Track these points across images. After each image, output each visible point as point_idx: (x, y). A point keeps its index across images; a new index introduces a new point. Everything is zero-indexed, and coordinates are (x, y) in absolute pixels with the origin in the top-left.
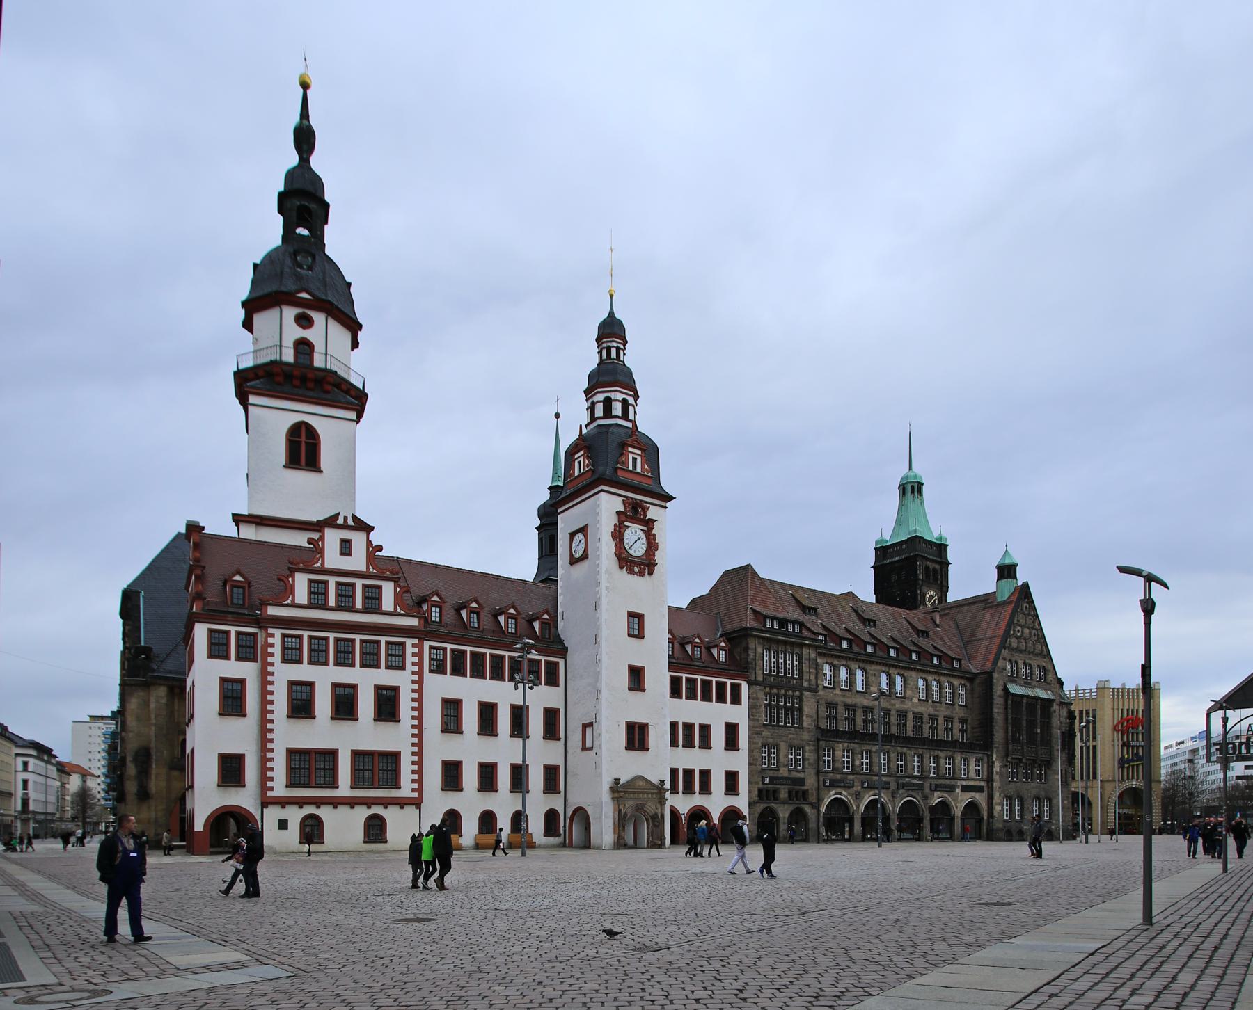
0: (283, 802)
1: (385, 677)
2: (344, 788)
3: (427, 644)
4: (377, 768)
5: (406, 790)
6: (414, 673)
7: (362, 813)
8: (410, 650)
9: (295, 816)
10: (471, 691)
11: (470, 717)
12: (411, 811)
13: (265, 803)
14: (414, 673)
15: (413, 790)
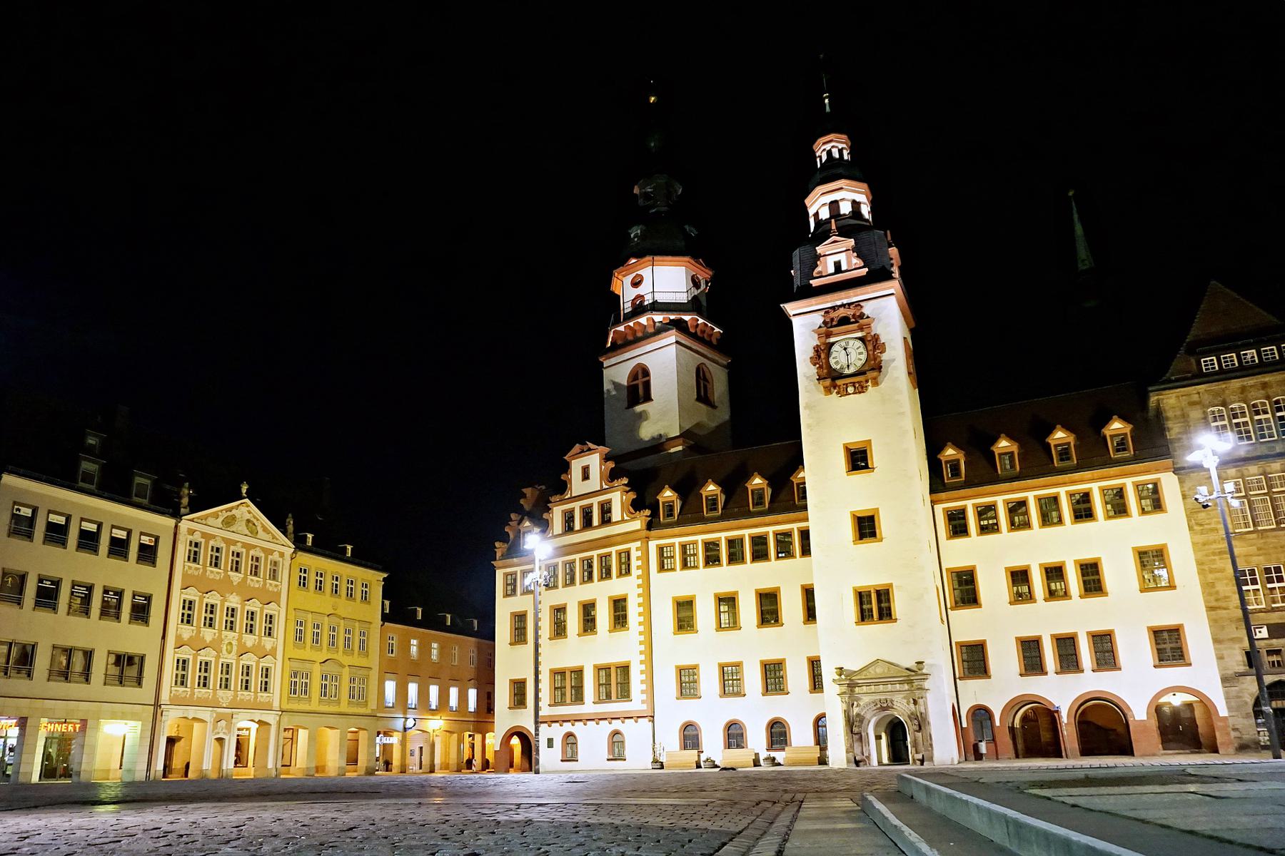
0: (552, 721)
1: (617, 586)
2: (589, 706)
3: (653, 545)
4: (616, 680)
5: (637, 702)
6: (639, 577)
7: (606, 728)
8: (635, 555)
9: (557, 732)
10: (704, 584)
11: (705, 612)
12: (644, 722)
13: (537, 723)
14: (639, 577)
15: (643, 702)
